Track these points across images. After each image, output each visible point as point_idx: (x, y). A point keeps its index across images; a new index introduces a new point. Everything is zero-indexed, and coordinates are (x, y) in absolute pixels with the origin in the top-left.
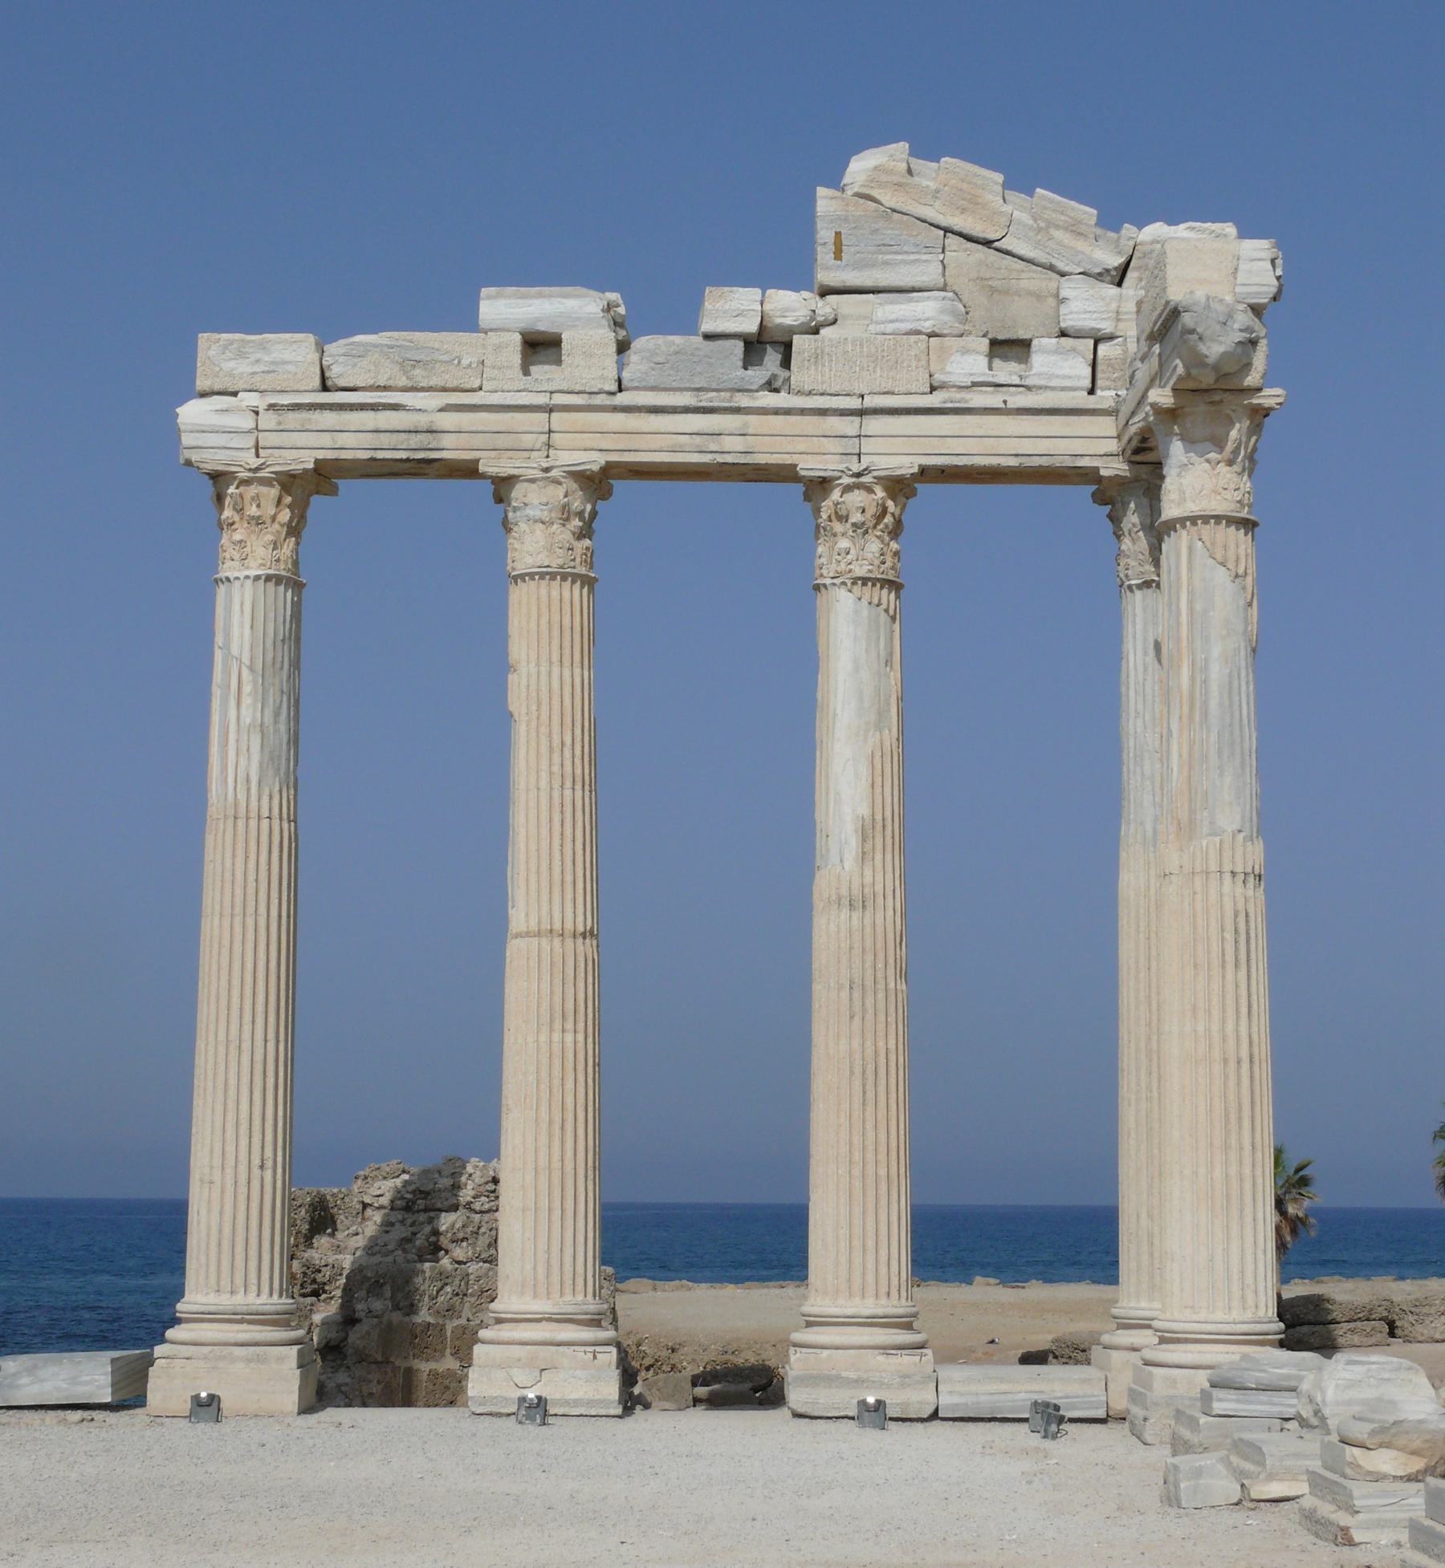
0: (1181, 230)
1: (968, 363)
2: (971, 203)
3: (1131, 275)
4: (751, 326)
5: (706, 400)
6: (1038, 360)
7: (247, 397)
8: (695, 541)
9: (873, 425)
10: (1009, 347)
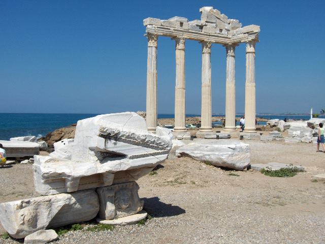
0: (234, 20)
1: (218, 32)
2: (218, 15)
3: (230, 24)
4: (200, 24)
5: (197, 32)
6: (223, 32)
7: (152, 24)
8: (196, 46)
9: (210, 37)
10: (221, 30)
